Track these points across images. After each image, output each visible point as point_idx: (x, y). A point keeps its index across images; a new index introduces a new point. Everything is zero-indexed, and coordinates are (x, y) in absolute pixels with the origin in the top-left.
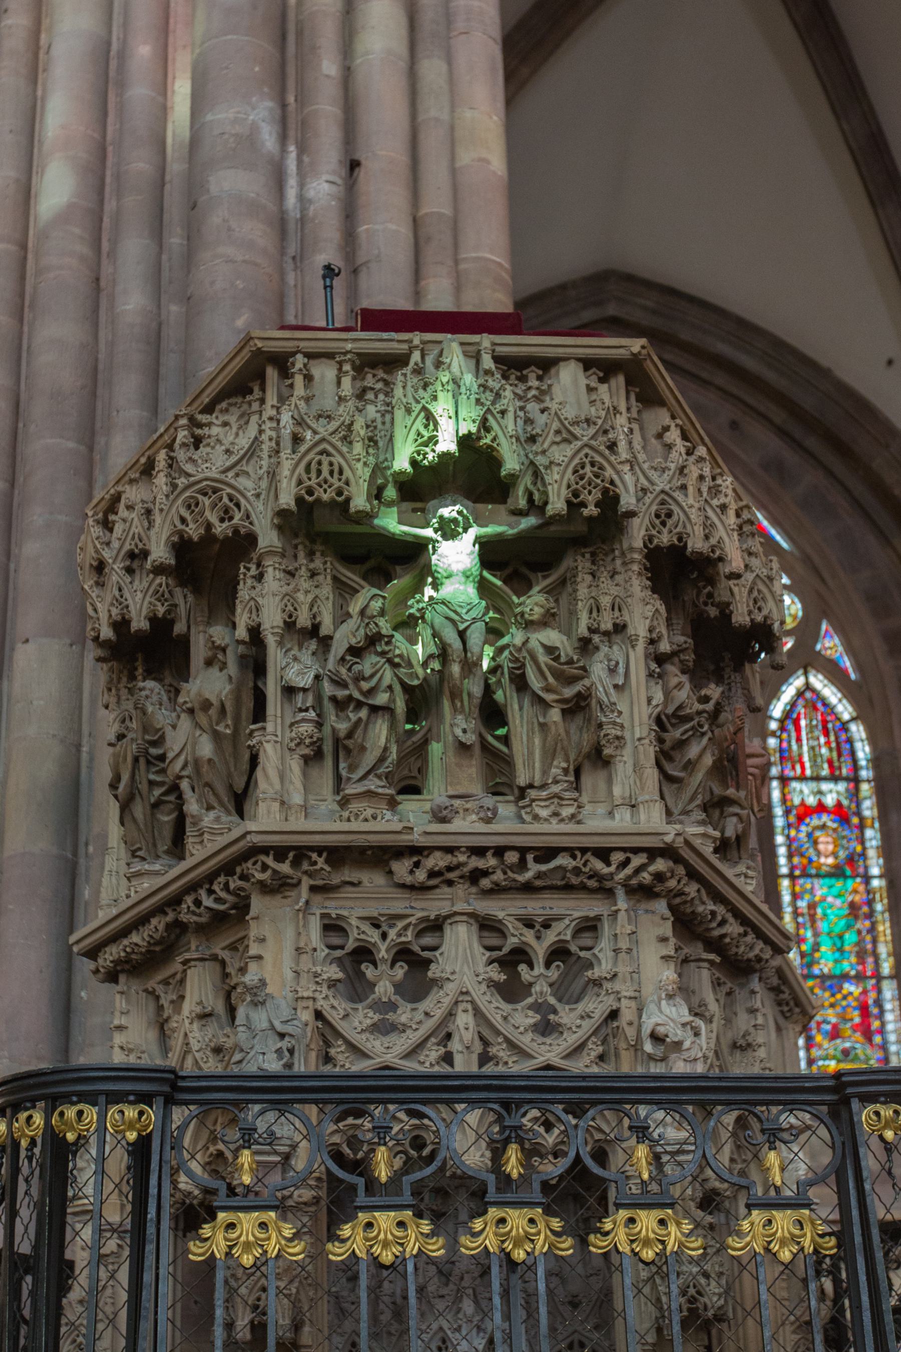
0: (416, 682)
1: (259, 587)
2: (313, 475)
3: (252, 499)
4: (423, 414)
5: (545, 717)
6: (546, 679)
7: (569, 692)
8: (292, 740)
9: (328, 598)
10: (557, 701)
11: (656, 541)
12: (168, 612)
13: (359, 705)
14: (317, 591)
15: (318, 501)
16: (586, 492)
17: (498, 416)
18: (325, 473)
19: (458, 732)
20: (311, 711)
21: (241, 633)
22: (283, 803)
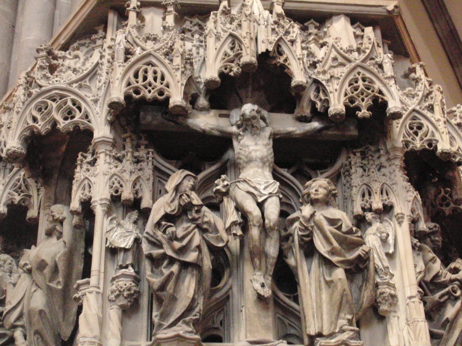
0: (221, 245)
1: (92, 169)
2: (140, 79)
3: (91, 103)
4: (230, 40)
5: (330, 275)
6: (330, 243)
7: (352, 256)
8: (112, 293)
9: (148, 179)
10: (342, 262)
11: (411, 146)
12: (23, 200)
13: (172, 261)
14: (140, 173)
15: (143, 99)
16: (360, 99)
17: (289, 44)
18: (150, 78)
19: (257, 286)
20: (130, 268)
21: (75, 205)
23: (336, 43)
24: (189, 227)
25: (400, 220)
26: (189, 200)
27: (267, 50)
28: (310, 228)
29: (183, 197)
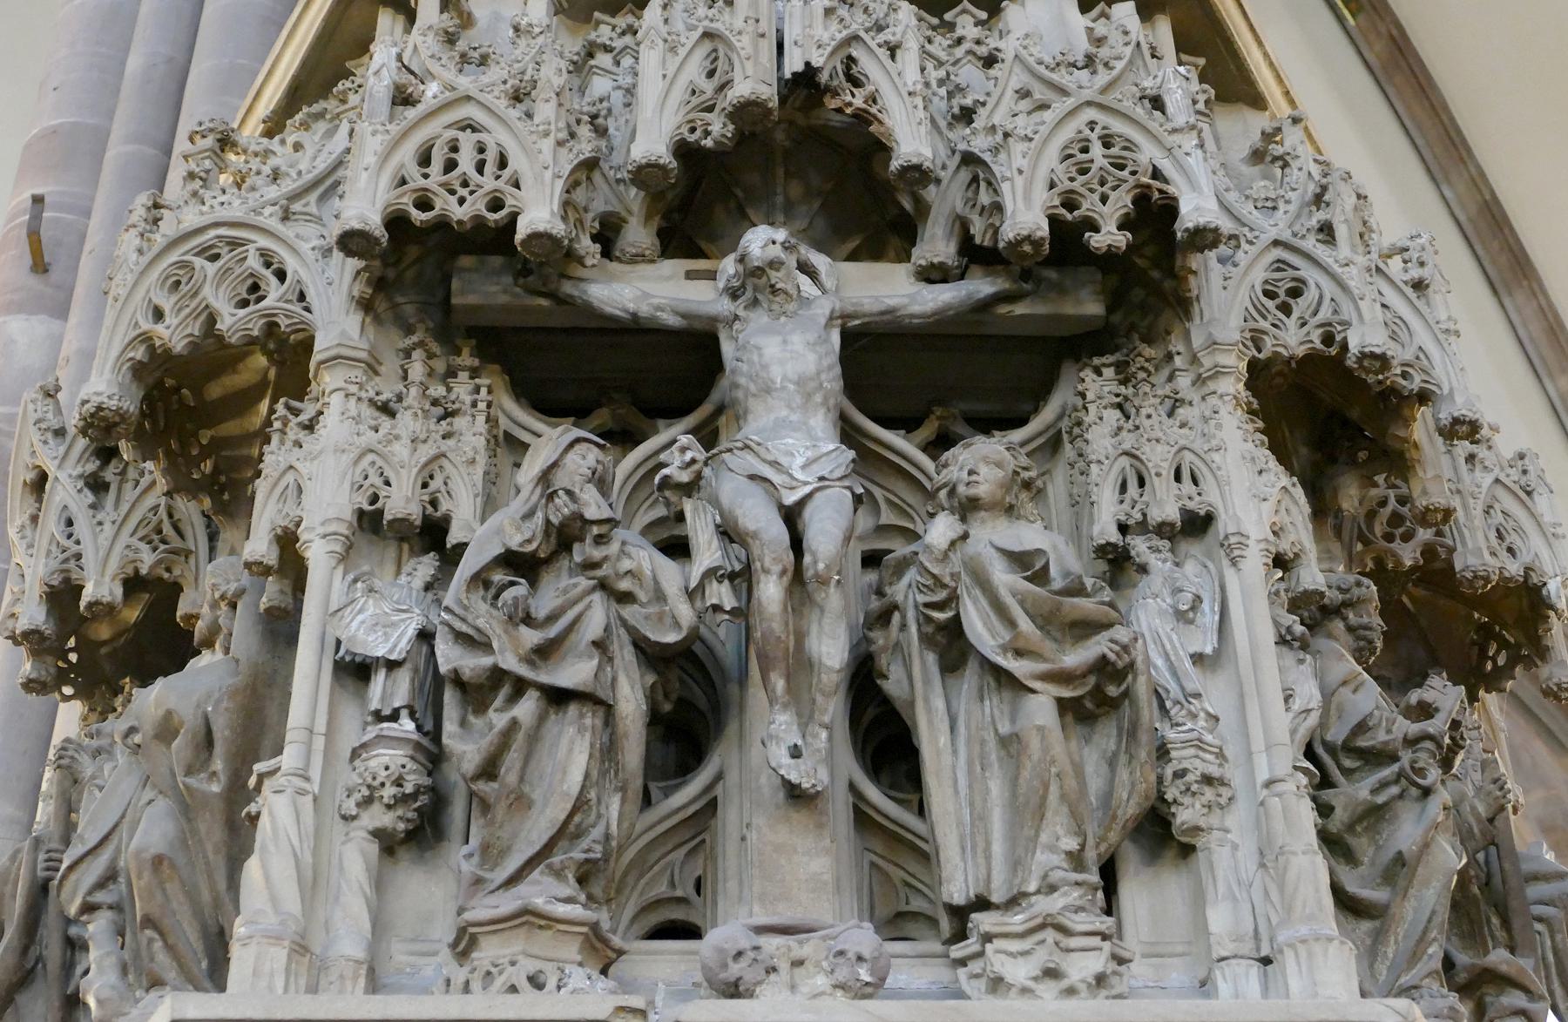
0: (671, 638)
6: (1011, 623)
7: (1076, 657)
9: (473, 462)
11: (1268, 342)
13: (520, 687)
15: (443, 224)
16: (1096, 197)
17: (883, 54)
19: (780, 755)
21: (259, 546)
22: (300, 948)
23: (1025, 48)
24: (575, 585)
25: (1236, 553)
26: (573, 507)
27: (808, 64)
28: (947, 580)
29: (557, 500)
